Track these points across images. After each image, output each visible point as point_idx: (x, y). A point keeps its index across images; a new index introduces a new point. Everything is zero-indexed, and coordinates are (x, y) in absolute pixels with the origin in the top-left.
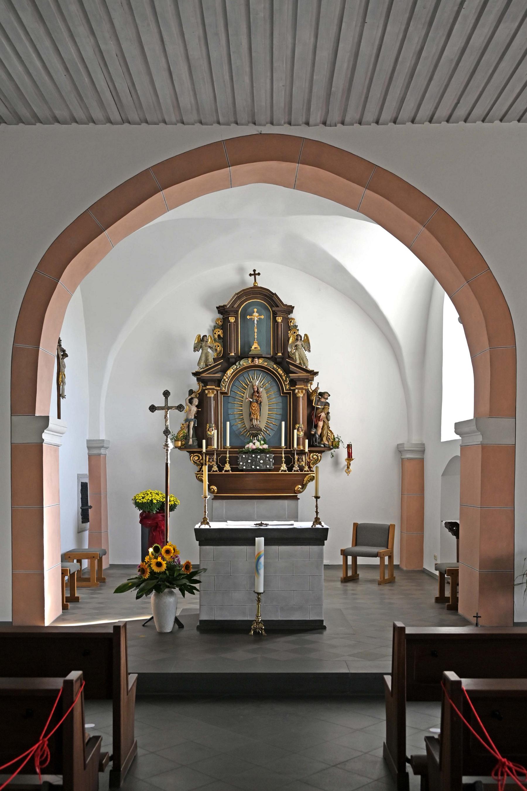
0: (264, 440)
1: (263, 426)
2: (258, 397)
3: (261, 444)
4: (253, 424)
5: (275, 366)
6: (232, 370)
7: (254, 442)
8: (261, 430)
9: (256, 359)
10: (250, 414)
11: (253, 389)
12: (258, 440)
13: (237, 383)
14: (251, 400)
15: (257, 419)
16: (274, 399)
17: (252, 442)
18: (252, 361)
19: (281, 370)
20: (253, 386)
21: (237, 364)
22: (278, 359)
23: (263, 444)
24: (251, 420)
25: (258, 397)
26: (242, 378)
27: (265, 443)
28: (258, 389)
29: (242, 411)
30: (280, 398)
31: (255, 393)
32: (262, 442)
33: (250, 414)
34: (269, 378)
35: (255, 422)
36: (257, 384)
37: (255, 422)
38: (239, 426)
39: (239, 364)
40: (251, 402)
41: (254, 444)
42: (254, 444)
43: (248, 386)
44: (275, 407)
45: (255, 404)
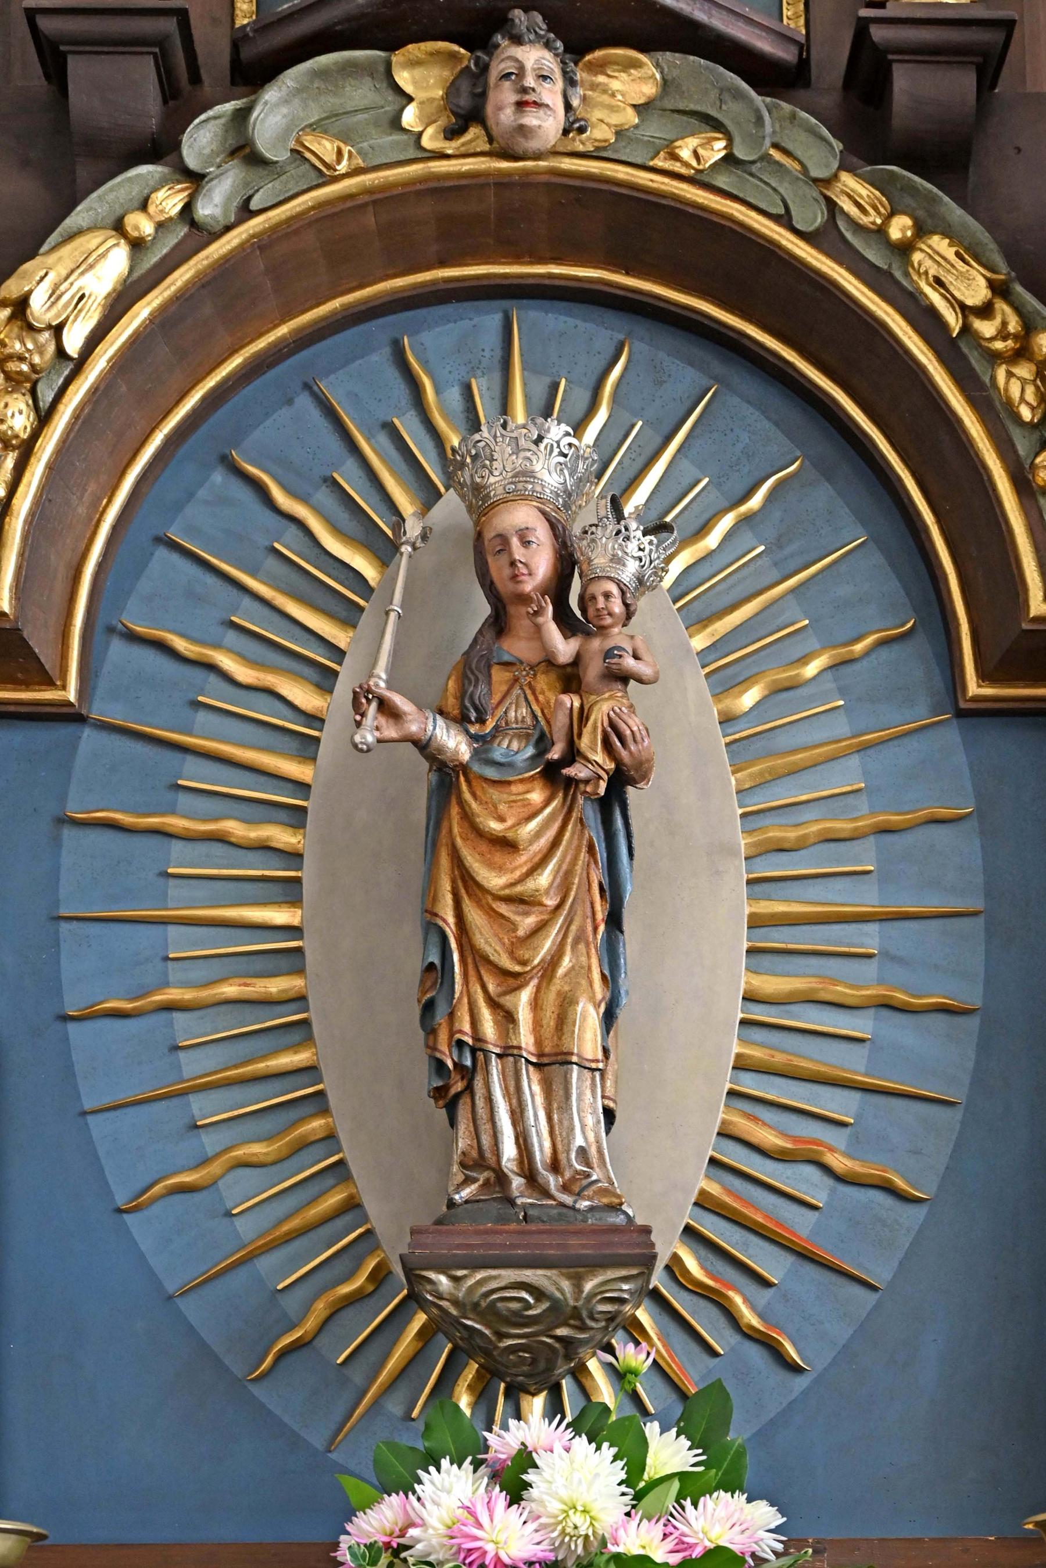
0: (700, 1416)
1: (661, 1183)
2: (570, 677)
3: (639, 1489)
4: (481, 1162)
5: (855, 193)
6: (115, 264)
7: (503, 1442)
8: (635, 1250)
9: (535, 57)
10: (437, 973)
11: (485, 551)
12: (591, 1425)
13: (209, 510)
14: (455, 743)
15: (554, 1062)
16: (847, 776)
17: (471, 1451)
18: (466, 113)
19: (970, 251)
20: (481, 504)
21: (200, 141)
22: (907, 84)
23: (691, 1488)
24: (454, 1087)
25: (570, 677)
26: (289, 425)
27: (722, 1471)
28: (566, 563)
29: (293, 960)
30: (952, 735)
31: (534, 637)
32: (669, 1453)
33: (437, 973)
34: (753, 419)
35: (515, 1121)
36: (550, 477)
37: (515, 1121)
38: (252, 1204)
39: (243, 151)
40: (446, 775)
41: (513, 1481)
42: (513, 1481)
43: (385, 550)
44: (866, 898)
45: (529, 815)
